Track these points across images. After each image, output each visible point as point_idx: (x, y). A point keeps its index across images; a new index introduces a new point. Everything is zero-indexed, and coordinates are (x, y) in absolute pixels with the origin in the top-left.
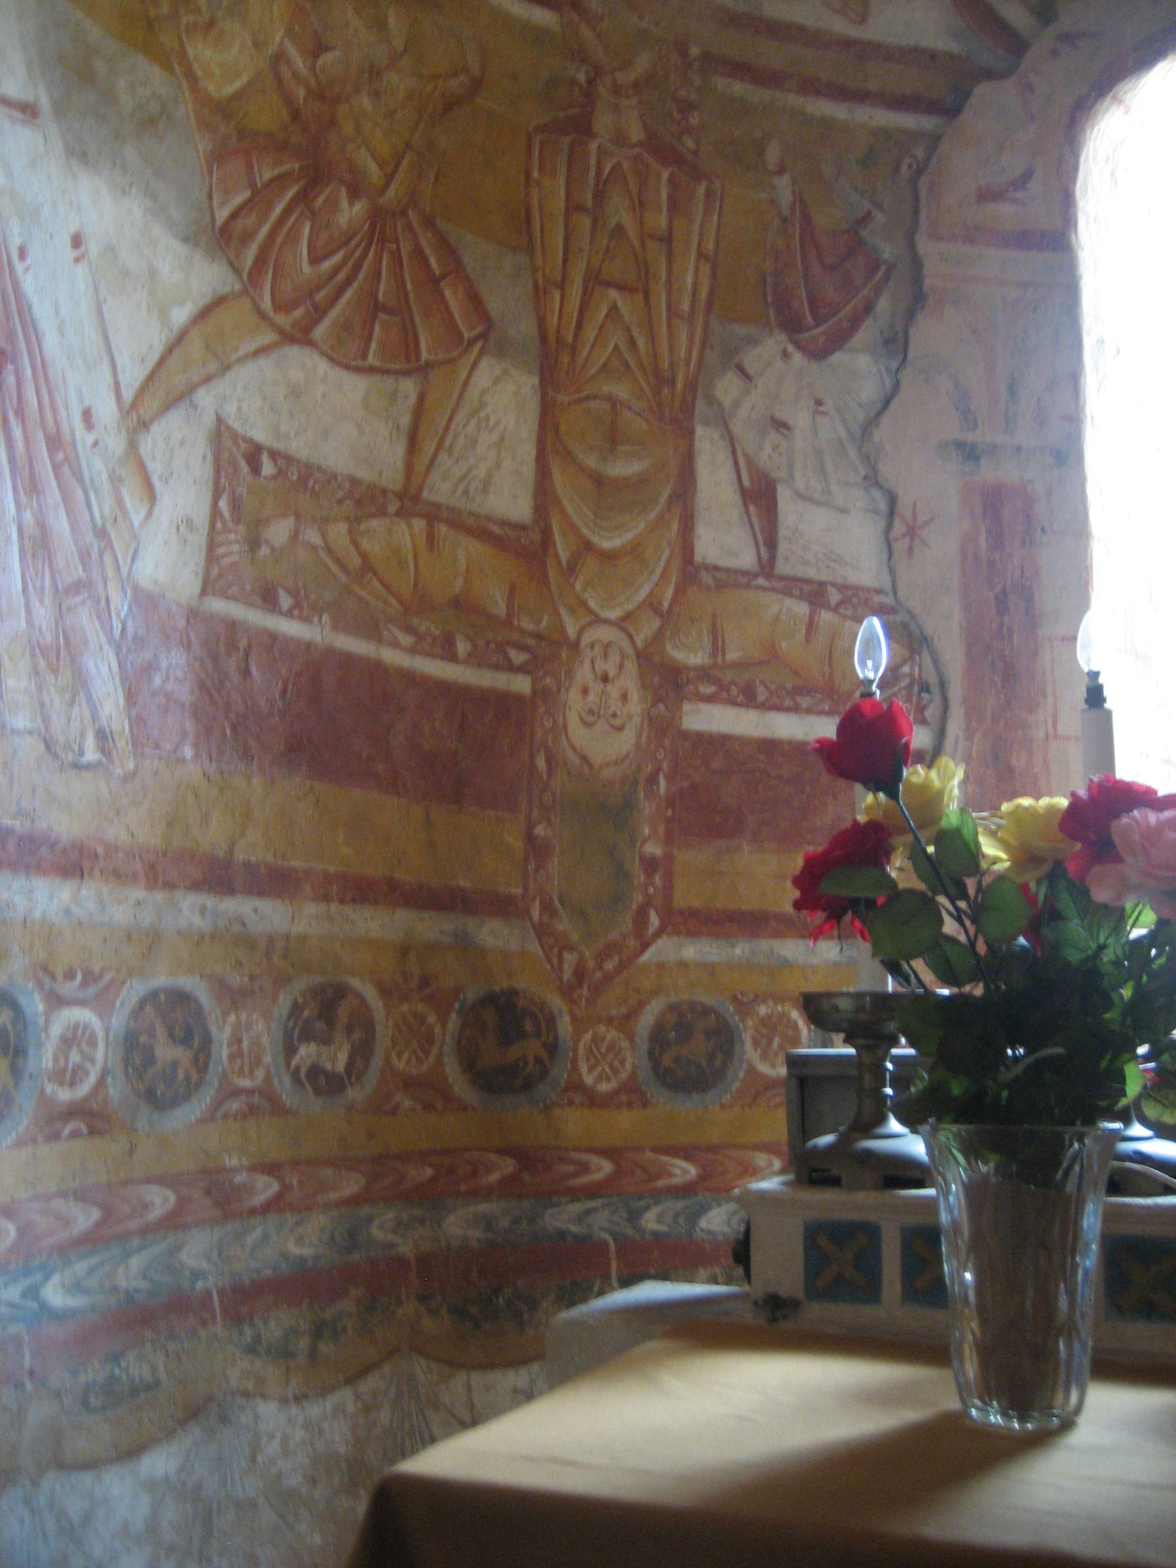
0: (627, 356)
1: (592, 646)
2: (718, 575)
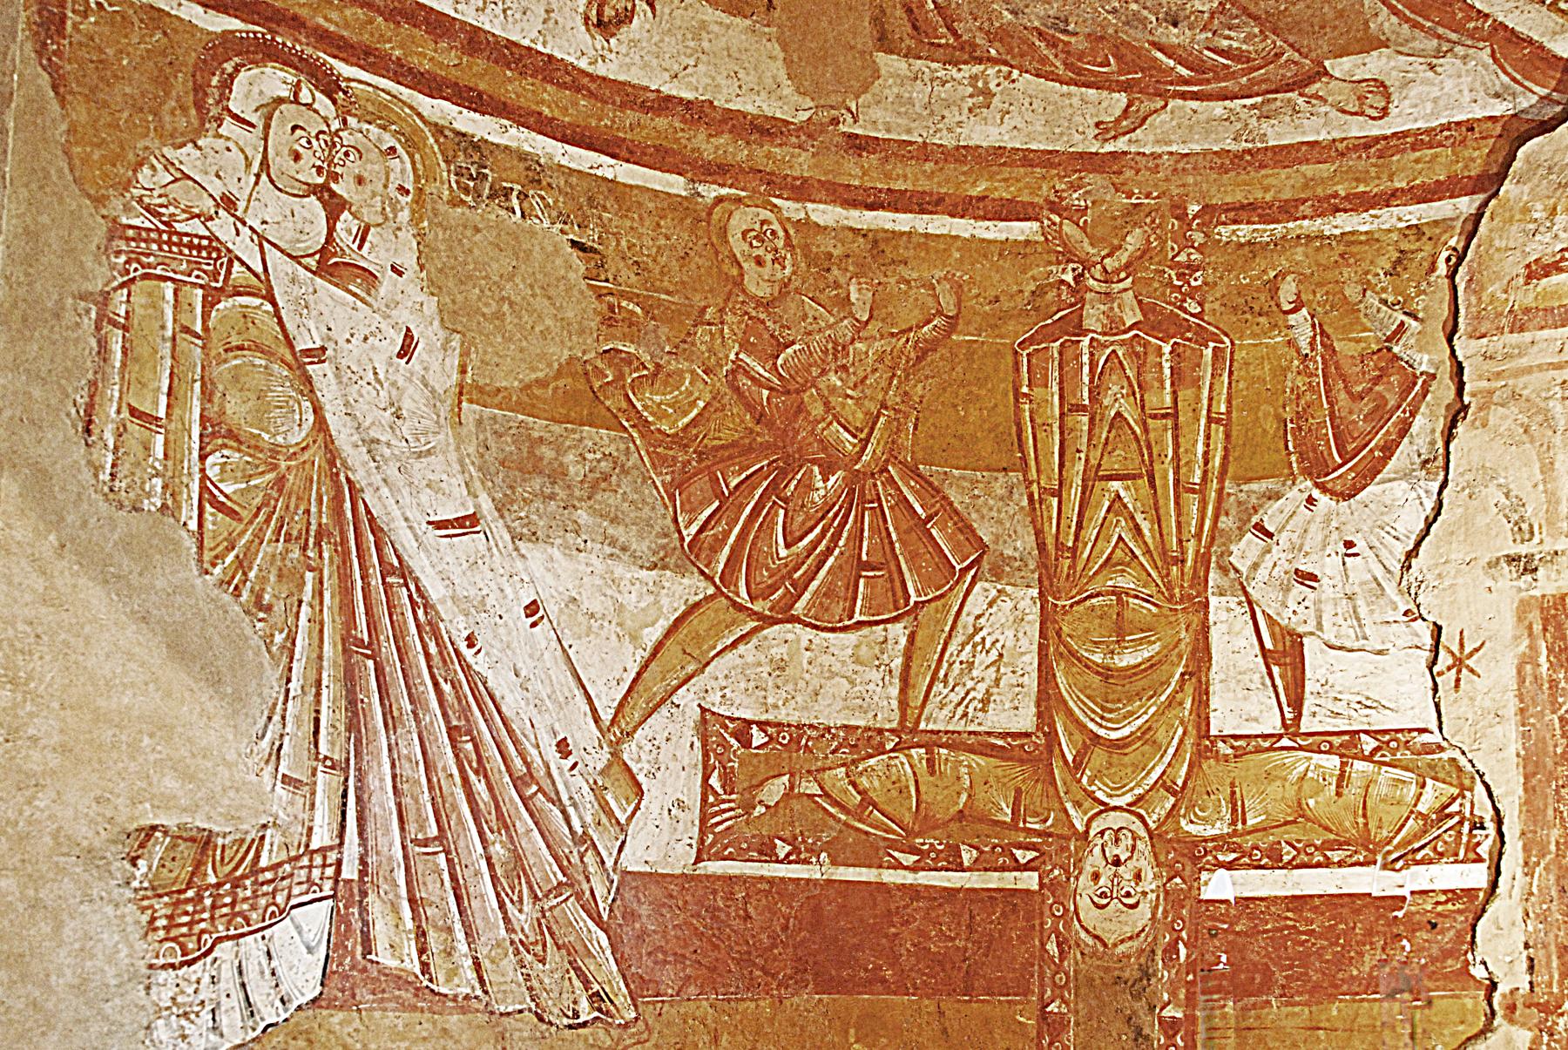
1: (1102, 833)
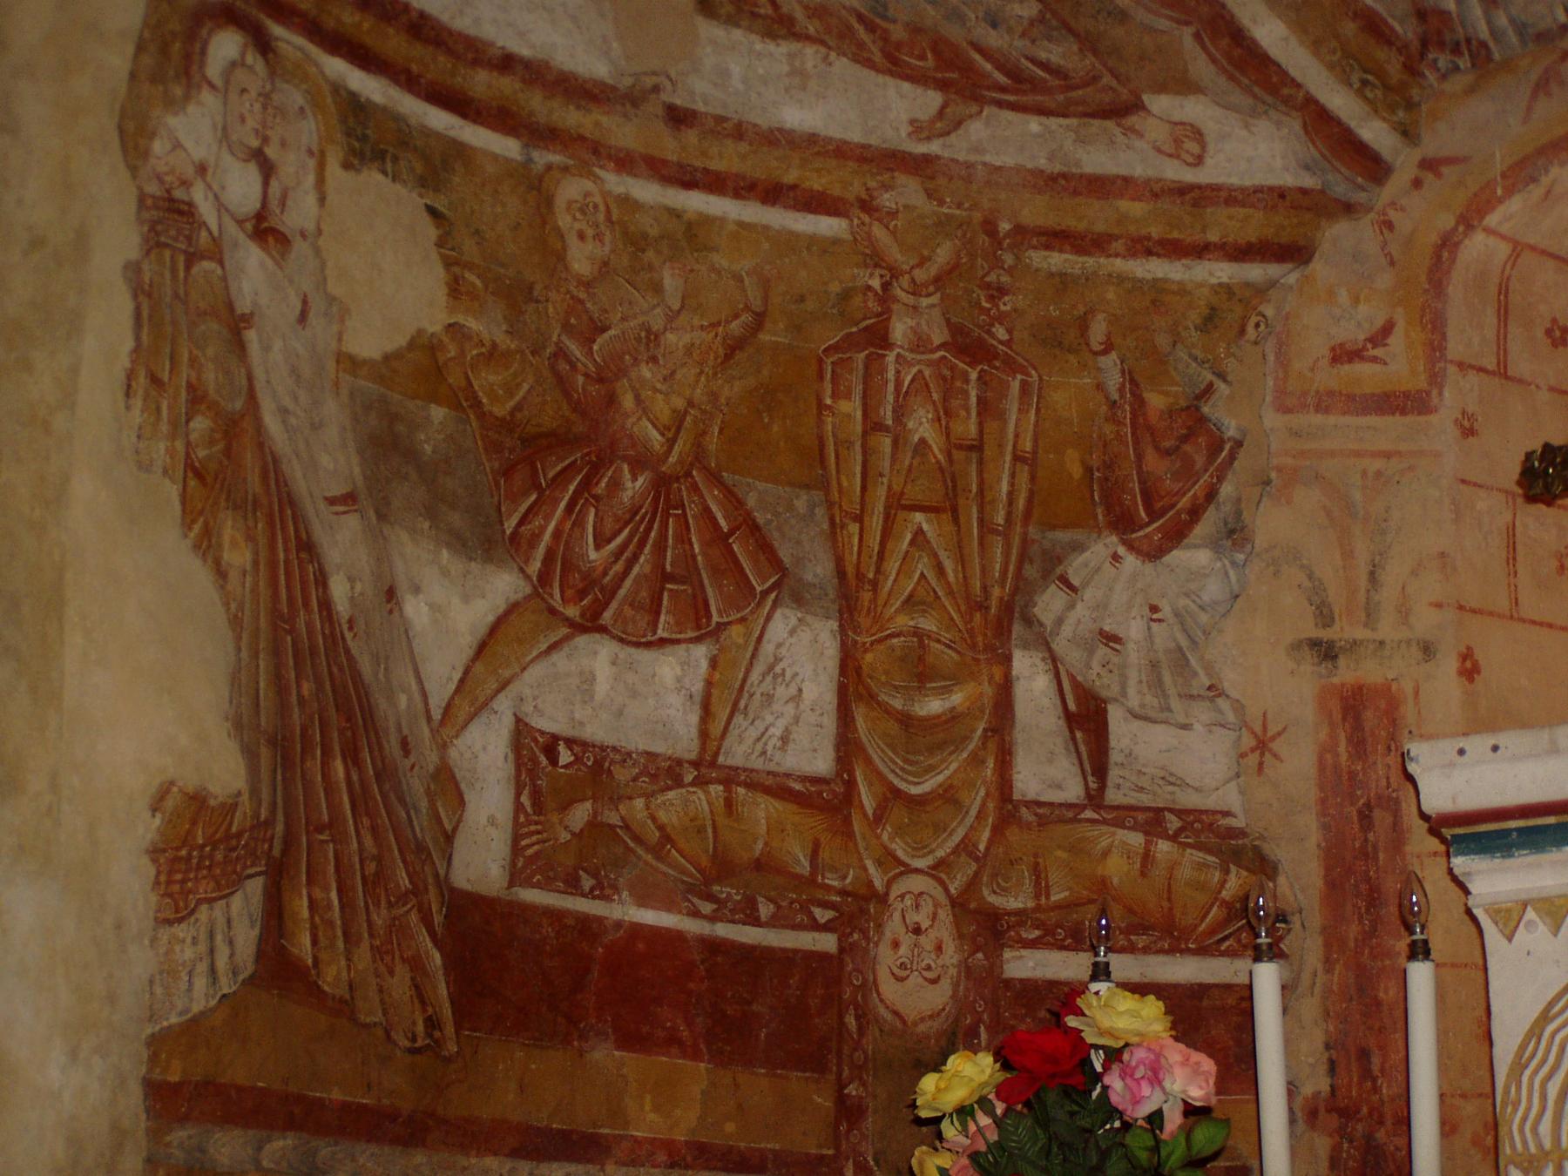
0: (934, 583)
1: (902, 896)
2: (1040, 811)
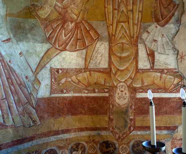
0: (125, 34)
2: (143, 71)
